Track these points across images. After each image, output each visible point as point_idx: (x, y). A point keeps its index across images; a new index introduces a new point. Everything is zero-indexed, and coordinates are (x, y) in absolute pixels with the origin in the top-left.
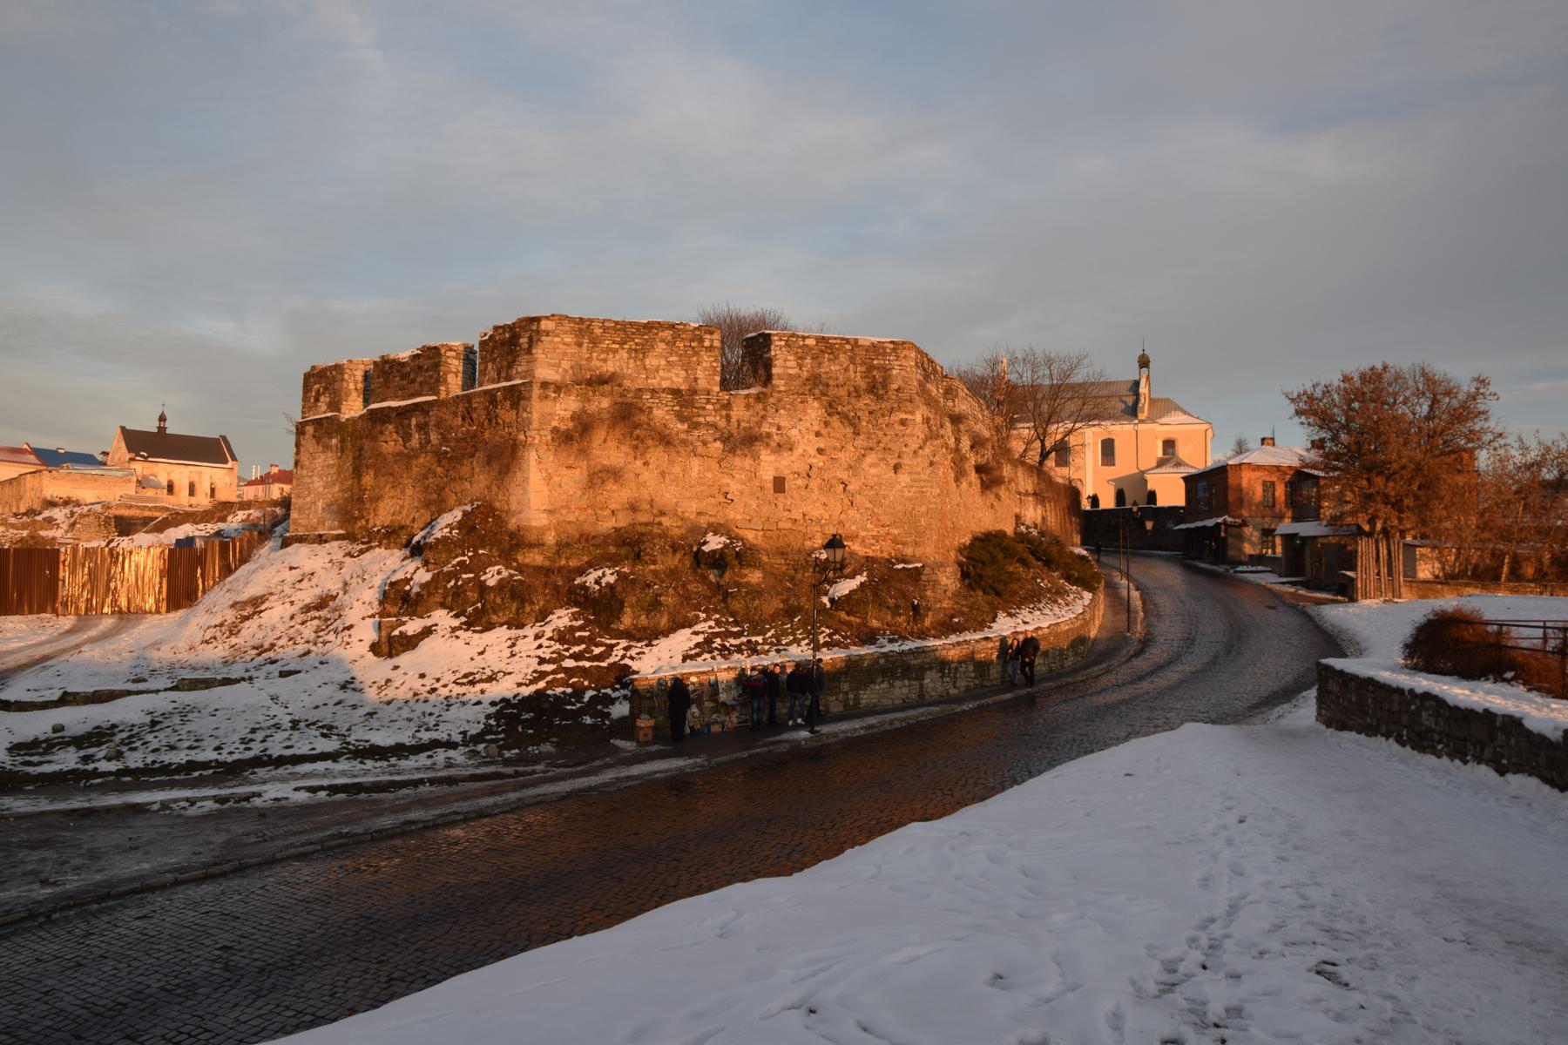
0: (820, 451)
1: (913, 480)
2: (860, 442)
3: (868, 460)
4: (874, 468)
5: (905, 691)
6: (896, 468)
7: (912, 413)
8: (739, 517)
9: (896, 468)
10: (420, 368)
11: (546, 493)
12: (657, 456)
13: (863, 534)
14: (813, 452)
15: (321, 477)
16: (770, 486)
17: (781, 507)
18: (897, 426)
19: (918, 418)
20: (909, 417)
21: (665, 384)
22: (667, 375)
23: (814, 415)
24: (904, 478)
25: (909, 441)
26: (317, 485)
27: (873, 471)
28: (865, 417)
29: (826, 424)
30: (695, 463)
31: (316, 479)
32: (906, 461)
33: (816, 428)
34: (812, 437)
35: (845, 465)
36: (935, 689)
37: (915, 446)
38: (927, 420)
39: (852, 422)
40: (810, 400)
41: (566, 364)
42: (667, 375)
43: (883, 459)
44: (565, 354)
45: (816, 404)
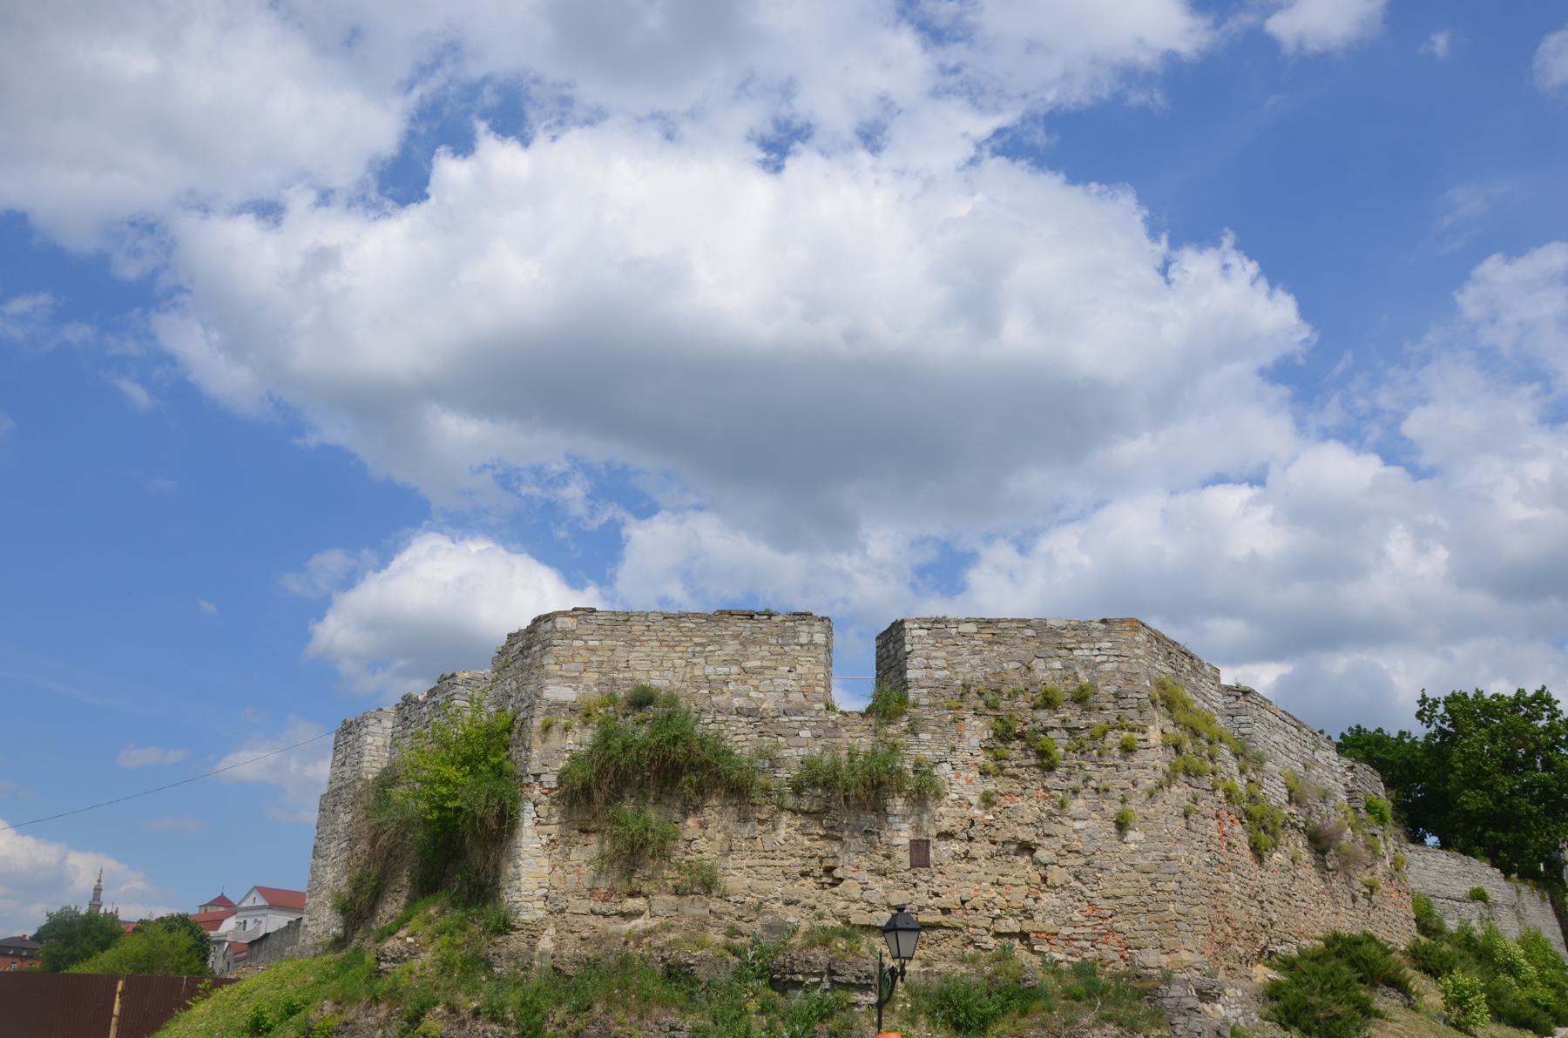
11: (546, 870)
13: (1066, 931)
16: (903, 856)
17: (923, 887)
19: (1154, 736)
21: (738, 702)
23: (975, 742)
32: (1136, 807)
33: (981, 760)
34: (974, 774)
37: (1151, 783)
40: (969, 716)
41: (591, 677)
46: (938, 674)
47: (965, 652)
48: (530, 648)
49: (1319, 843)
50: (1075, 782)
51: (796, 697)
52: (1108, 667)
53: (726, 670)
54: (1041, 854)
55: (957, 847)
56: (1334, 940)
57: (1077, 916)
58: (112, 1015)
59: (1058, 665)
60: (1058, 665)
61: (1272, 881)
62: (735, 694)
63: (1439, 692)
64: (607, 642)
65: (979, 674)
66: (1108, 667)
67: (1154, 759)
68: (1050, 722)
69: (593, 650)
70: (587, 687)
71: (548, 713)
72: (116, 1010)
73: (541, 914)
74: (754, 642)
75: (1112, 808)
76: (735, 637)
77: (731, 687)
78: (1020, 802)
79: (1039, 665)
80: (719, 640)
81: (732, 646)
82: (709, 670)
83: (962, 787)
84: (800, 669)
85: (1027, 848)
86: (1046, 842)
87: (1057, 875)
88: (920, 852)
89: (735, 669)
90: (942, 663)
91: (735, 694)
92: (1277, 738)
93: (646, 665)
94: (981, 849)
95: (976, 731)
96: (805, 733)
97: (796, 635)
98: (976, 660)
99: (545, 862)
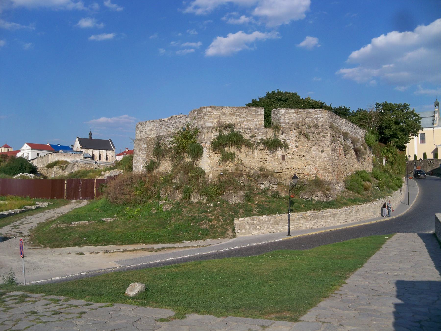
0: (297, 147)
1: (328, 155)
2: (310, 143)
3: (312, 149)
4: (314, 152)
5: (322, 223)
6: (322, 151)
7: (327, 134)
8: (270, 168)
9: (322, 151)
10: (171, 123)
11: (209, 162)
12: (244, 149)
13: (311, 173)
14: (294, 147)
15: (142, 157)
16: (281, 158)
17: (284, 164)
18: (322, 138)
19: (329, 135)
20: (326, 135)
21: (246, 127)
22: (247, 123)
23: (294, 135)
24: (324, 155)
25: (326, 142)
26: (140, 159)
27: (314, 152)
28: (311, 134)
29: (299, 138)
30: (256, 151)
31: (140, 158)
32: (325, 149)
33: (295, 139)
34: (294, 142)
35: (305, 151)
36: (332, 223)
38: (332, 136)
39: (306, 136)
40: (293, 130)
42: (247, 123)
43: (317, 149)
44: (215, 118)
45: (295, 131)
46: (287, 121)
47: (292, 116)
48: (200, 113)
49: (357, 151)
50: (314, 143)
51: (258, 126)
52: (321, 120)
53: (243, 120)
54: (307, 158)
55: (290, 157)
56: (357, 172)
57: (313, 170)
58: (64, 189)
59: (311, 119)
60: (311, 119)
61: (346, 160)
62: (245, 125)
63: (380, 102)
64: (218, 114)
65: (295, 121)
66: (321, 120)
67: (329, 139)
68: (309, 131)
69: (215, 115)
70: (215, 123)
71: (207, 129)
72: (65, 188)
73: (209, 171)
74: (250, 114)
75: (321, 149)
76: (245, 112)
77: (245, 123)
78: (303, 148)
79: (307, 119)
80: (242, 113)
81: (245, 114)
82: (240, 120)
83: (292, 145)
84: (259, 120)
85: (303, 156)
86: (307, 156)
87: (310, 162)
88: (283, 158)
89: (245, 120)
90: (287, 119)
91: (245, 125)
92: (349, 129)
93: (226, 118)
94: (295, 157)
95: (295, 133)
96: (260, 133)
97: (258, 112)
98: (294, 118)
99: (209, 160)
